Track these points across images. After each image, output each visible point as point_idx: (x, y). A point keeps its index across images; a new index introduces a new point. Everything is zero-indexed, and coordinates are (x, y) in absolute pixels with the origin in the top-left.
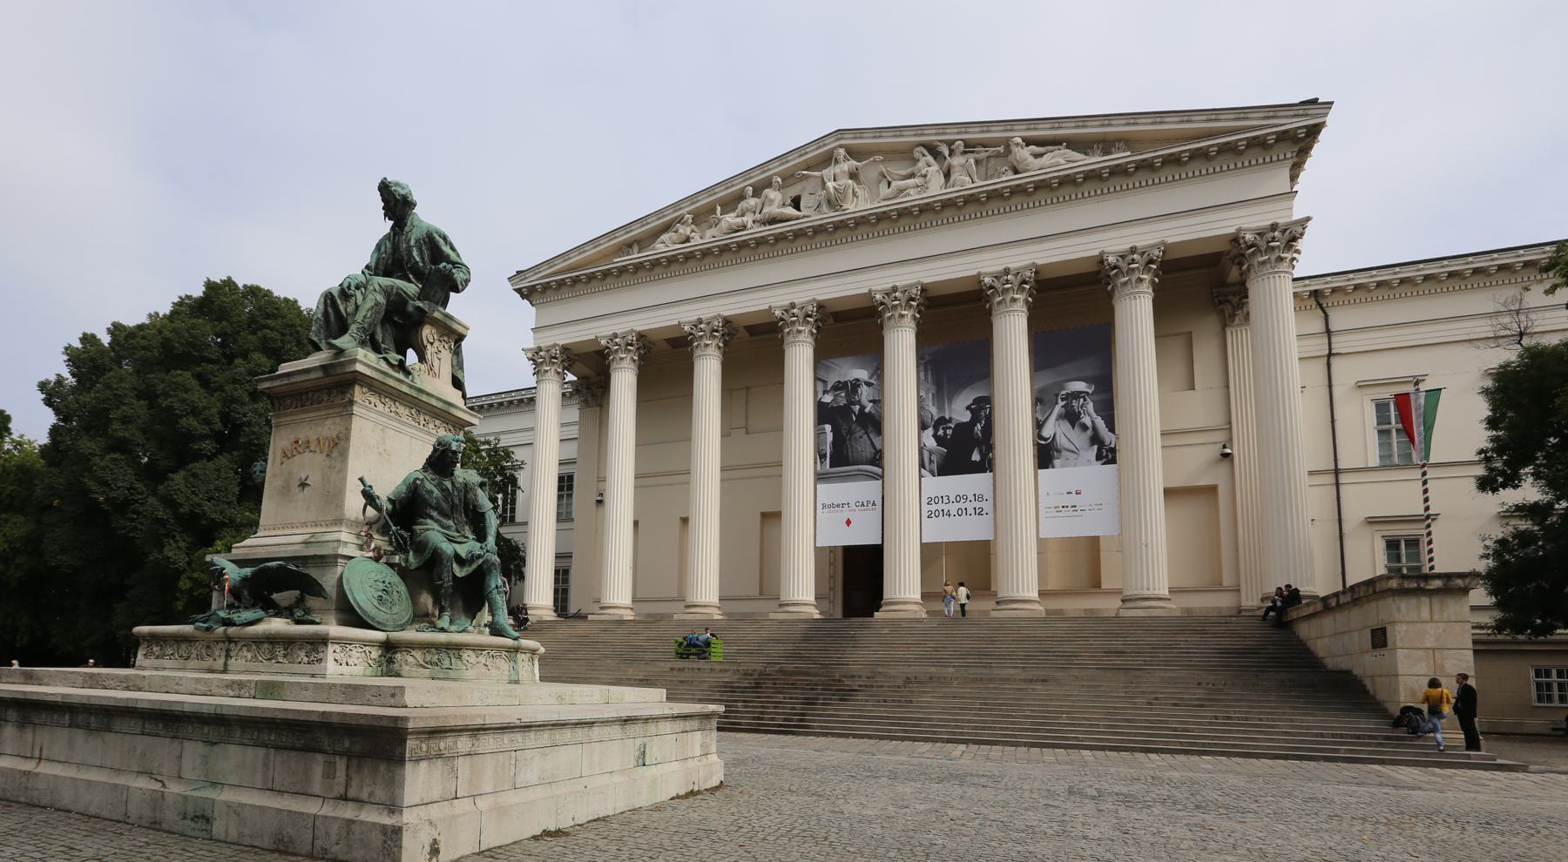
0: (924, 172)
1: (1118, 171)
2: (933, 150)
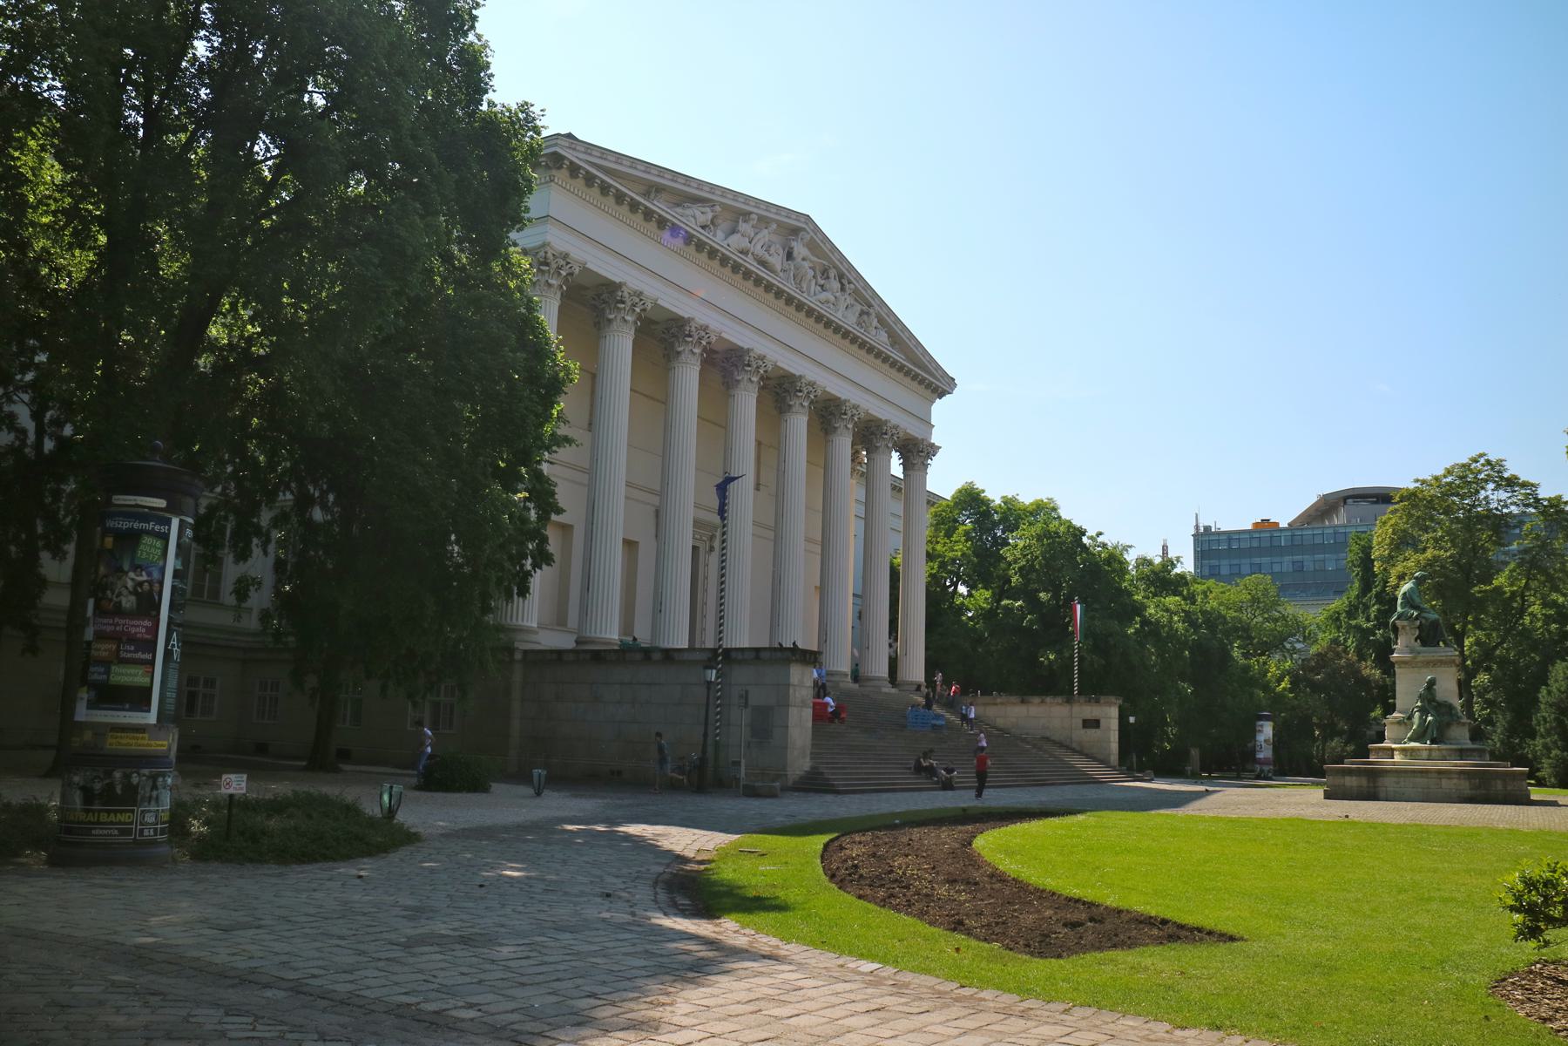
0: (837, 294)
1: (901, 368)
2: (841, 276)
